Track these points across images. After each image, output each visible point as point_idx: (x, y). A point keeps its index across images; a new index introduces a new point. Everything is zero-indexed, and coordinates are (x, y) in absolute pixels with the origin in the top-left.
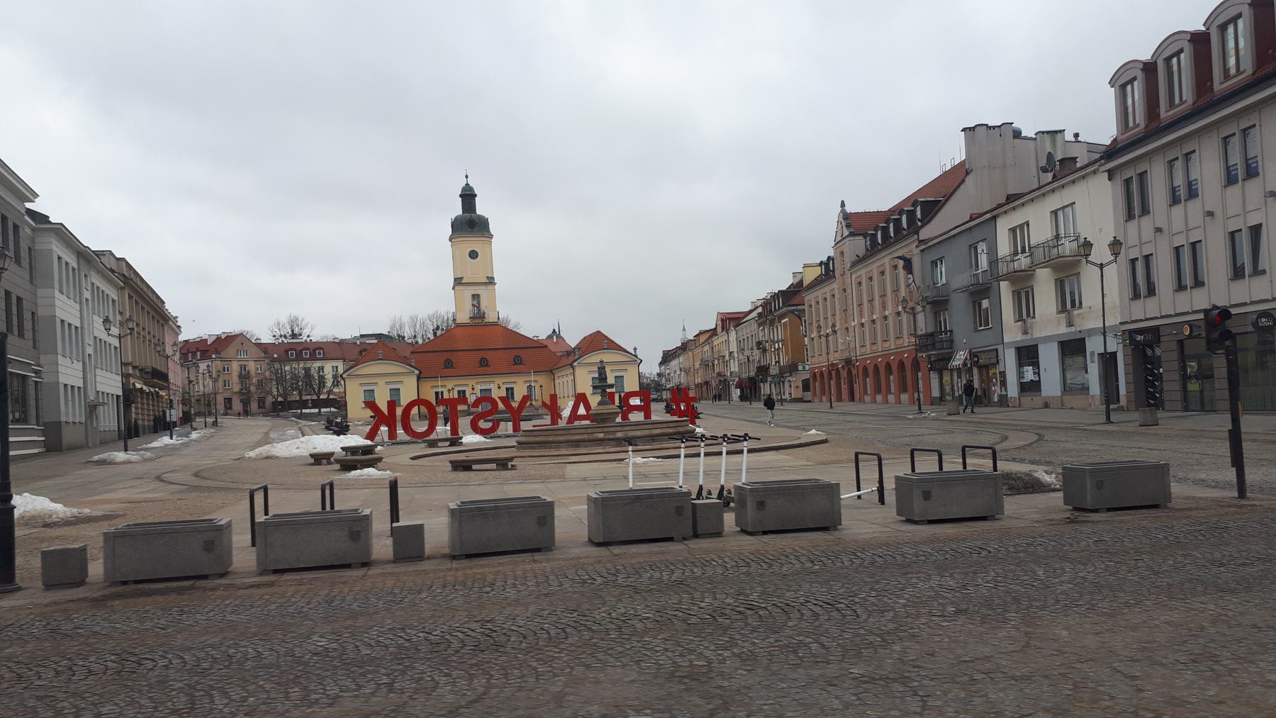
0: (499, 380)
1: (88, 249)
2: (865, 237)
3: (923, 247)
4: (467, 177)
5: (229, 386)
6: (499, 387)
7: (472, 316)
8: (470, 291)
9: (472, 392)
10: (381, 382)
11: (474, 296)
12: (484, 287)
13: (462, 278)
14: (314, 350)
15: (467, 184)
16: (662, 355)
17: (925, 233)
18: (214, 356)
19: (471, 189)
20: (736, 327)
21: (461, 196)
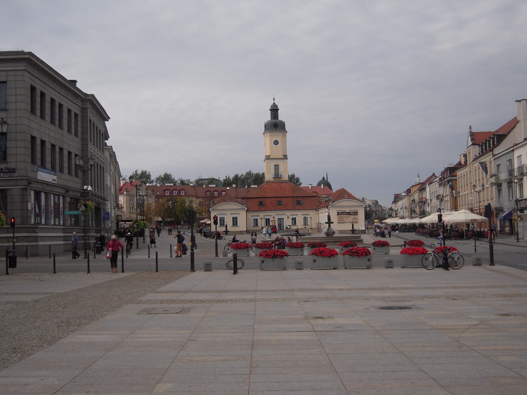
0: (289, 213)
1: (114, 154)
2: (479, 146)
3: (494, 158)
4: (274, 99)
5: (132, 211)
6: (288, 217)
7: (274, 177)
8: (273, 163)
9: (273, 219)
10: (228, 213)
11: (275, 166)
12: (281, 161)
13: (269, 156)
14: (180, 191)
15: (274, 104)
16: (394, 197)
17: (497, 151)
18: (125, 193)
19: (276, 106)
20: (429, 184)
21: (270, 110)
